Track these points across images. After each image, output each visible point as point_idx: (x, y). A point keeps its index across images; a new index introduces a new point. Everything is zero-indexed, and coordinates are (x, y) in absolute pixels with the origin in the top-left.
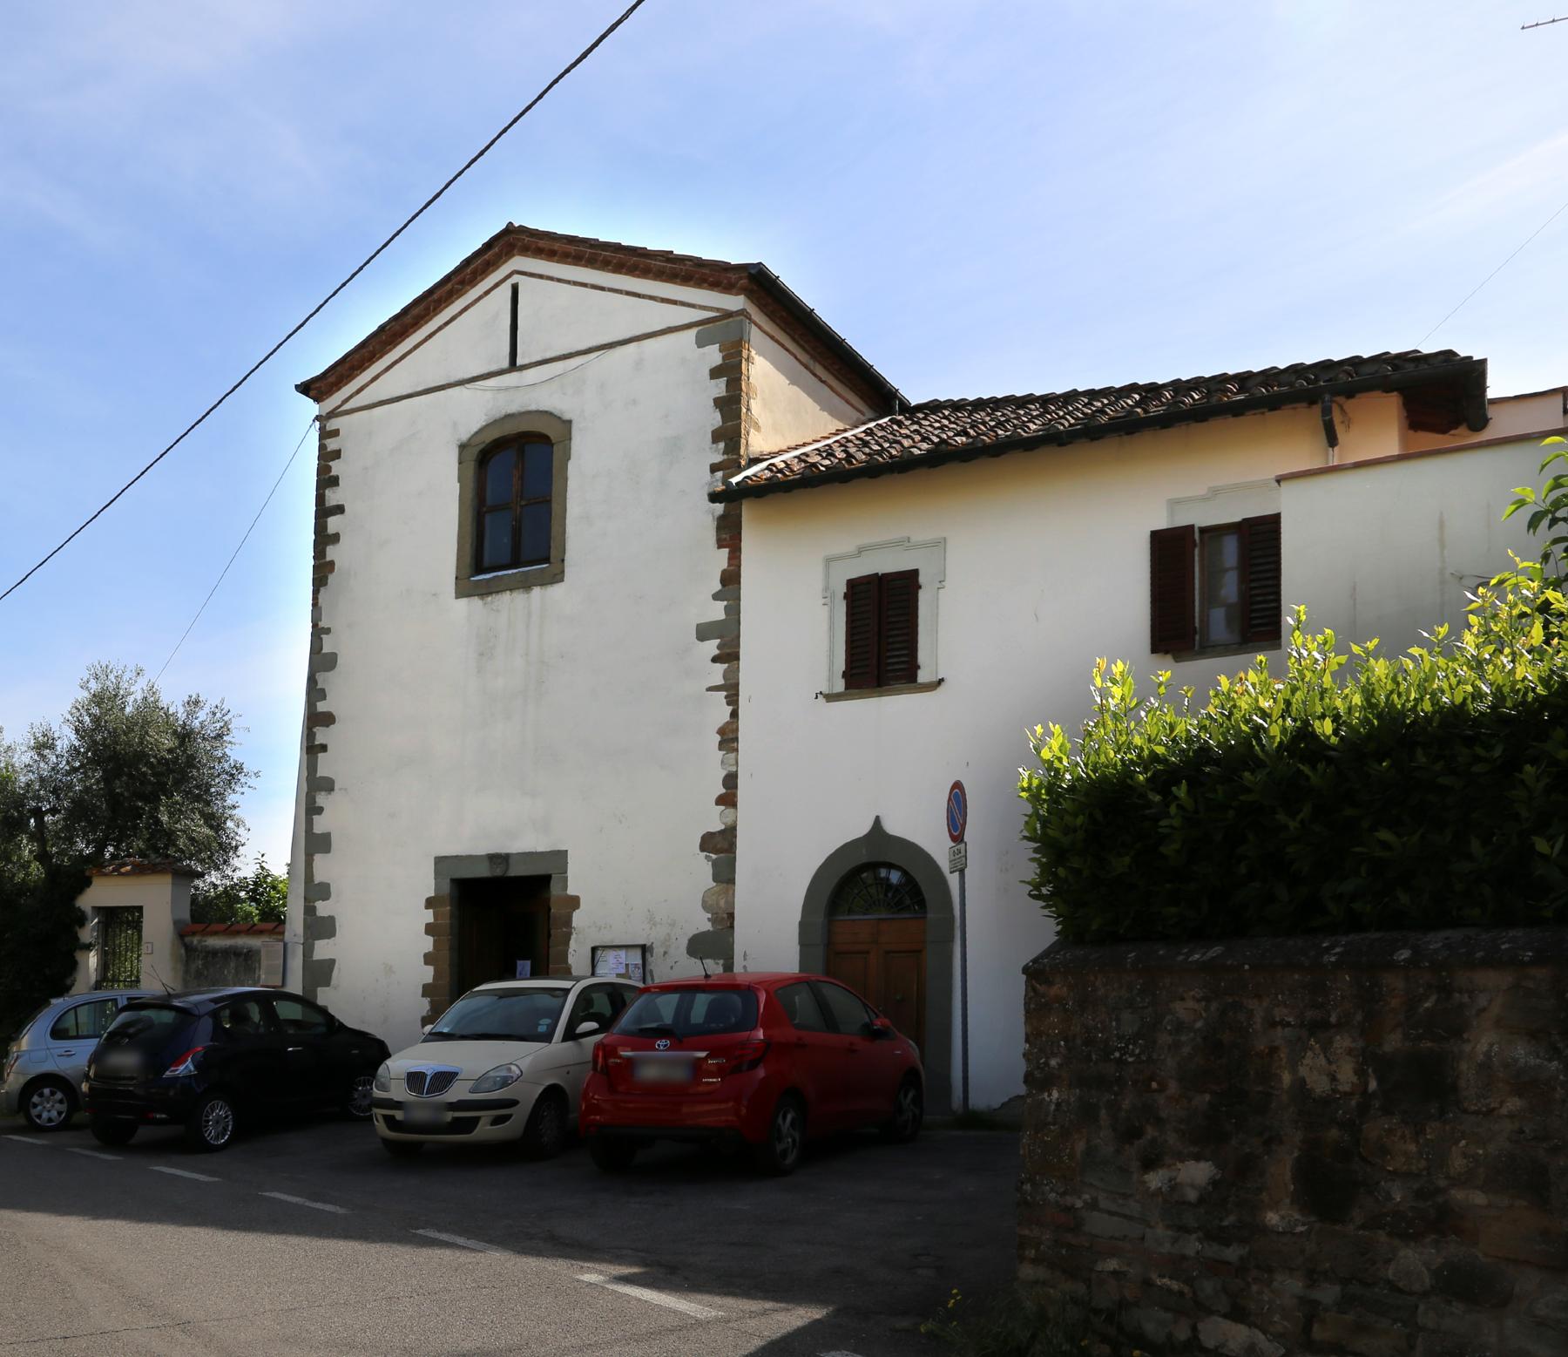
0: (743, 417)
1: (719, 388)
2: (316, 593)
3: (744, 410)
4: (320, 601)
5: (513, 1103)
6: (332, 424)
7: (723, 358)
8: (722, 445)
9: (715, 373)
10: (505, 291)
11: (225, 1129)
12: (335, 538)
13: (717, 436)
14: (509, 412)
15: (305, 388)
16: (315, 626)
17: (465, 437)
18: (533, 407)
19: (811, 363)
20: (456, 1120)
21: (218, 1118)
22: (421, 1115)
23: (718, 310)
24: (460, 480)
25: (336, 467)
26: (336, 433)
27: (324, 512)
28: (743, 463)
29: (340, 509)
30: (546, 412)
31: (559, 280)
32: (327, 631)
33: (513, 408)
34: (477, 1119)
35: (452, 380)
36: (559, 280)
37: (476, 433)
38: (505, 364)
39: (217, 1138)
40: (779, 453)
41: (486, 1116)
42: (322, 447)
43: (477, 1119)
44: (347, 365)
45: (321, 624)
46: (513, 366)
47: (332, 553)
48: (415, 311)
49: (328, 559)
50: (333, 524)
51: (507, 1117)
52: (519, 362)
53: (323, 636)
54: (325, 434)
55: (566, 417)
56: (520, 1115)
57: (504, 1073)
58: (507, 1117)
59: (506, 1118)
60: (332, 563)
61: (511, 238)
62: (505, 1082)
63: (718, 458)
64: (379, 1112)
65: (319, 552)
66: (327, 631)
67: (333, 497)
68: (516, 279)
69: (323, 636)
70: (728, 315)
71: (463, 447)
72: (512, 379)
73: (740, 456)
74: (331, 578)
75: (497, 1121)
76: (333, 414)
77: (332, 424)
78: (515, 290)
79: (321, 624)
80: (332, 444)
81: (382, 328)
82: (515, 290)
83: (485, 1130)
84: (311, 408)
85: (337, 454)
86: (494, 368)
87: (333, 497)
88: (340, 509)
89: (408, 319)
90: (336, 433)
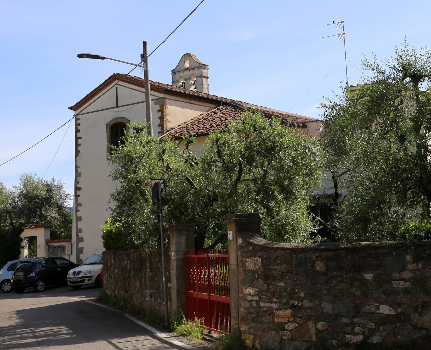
0: (164, 121)
1: (159, 114)
2: (76, 158)
3: (165, 120)
4: (77, 160)
5: (92, 276)
6: (78, 117)
7: (160, 108)
8: (160, 127)
9: (159, 111)
10: (115, 88)
11: (43, 287)
12: (80, 145)
13: (159, 125)
14: (117, 117)
15: (71, 108)
16: (76, 166)
17: (107, 122)
18: (121, 116)
19: (190, 101)
20: (81, 280)
21: (41, 285)
22: (75, 280)
23: (158, 97)
24: (107, 132)
25: (79, 128)
26: (79, 119)
27: (77, 138)
28: (165, 131)
29: (80, 138)
30: (124, 118)
31: (126, 87)
32: (79, 167)
33: (117, 116)
34: (85, 280)
35: (104, 108)
36: (126, 87)
37: (110, 122)
38: (115, 106)
39: (41, 289)
40: (175, 127)
41: (87, 279)
42: (76, 122)
43: (85, 280)
44: (80, 103)
45: (77, 166)
46: (117, 106)
47: (79, 148)
48: (95, 92)
49: (78, 150)
50: (79, 141)
51: (91, 279)
52: (118, 105)
53: (78, 169)
54: (76, 119)
55: (129, 119)
56: (94, 279)
57: (90, 271)
58: (91, 279)
59: (91, 279)
60: (79, 151)
61: (114, 77)
62: (90, 272)
63: (160, 130)
64: (68, 280)
65: (76, 148)
66: (79, 167)
67: (79, 135)
68: (117, 86)
69: (78, 169)
70: (161, 98)
71: (107, 125)
72: (117, 109)
73: (164, 130)
74: (79, 154)
75: (89, 280)
76: (78, 114)
77: (78, 117)
78: (117, 88)
79: (77, 166)
80: (78, 122)
81: (87, 95)
82: (117, 88)
83: (86, 282)
84: (73, 112)
85: (79, 124)
86: (113, 106)
87: (79, 135)
88: (80, 138)
89: (93, 93)
90: (79, 119)
